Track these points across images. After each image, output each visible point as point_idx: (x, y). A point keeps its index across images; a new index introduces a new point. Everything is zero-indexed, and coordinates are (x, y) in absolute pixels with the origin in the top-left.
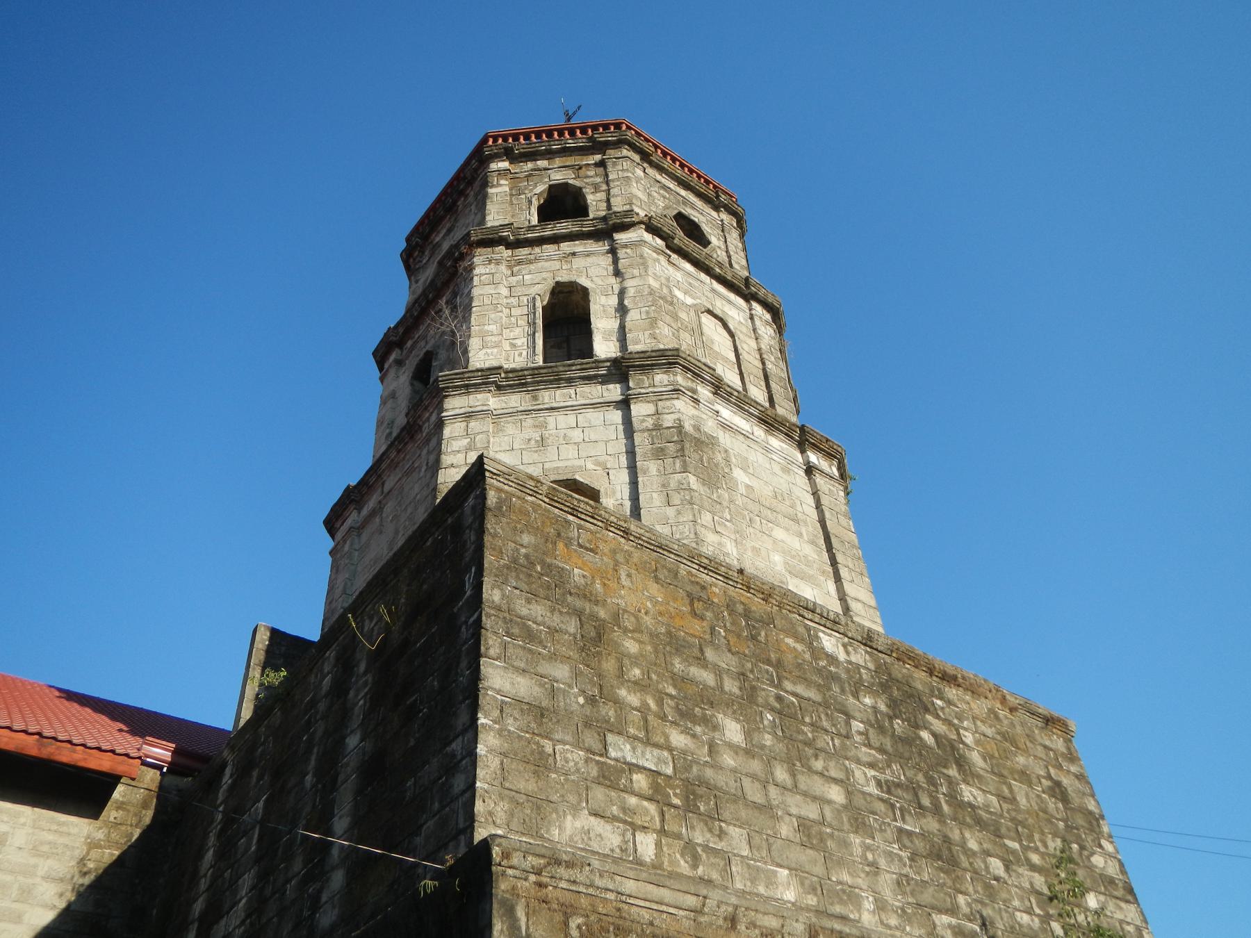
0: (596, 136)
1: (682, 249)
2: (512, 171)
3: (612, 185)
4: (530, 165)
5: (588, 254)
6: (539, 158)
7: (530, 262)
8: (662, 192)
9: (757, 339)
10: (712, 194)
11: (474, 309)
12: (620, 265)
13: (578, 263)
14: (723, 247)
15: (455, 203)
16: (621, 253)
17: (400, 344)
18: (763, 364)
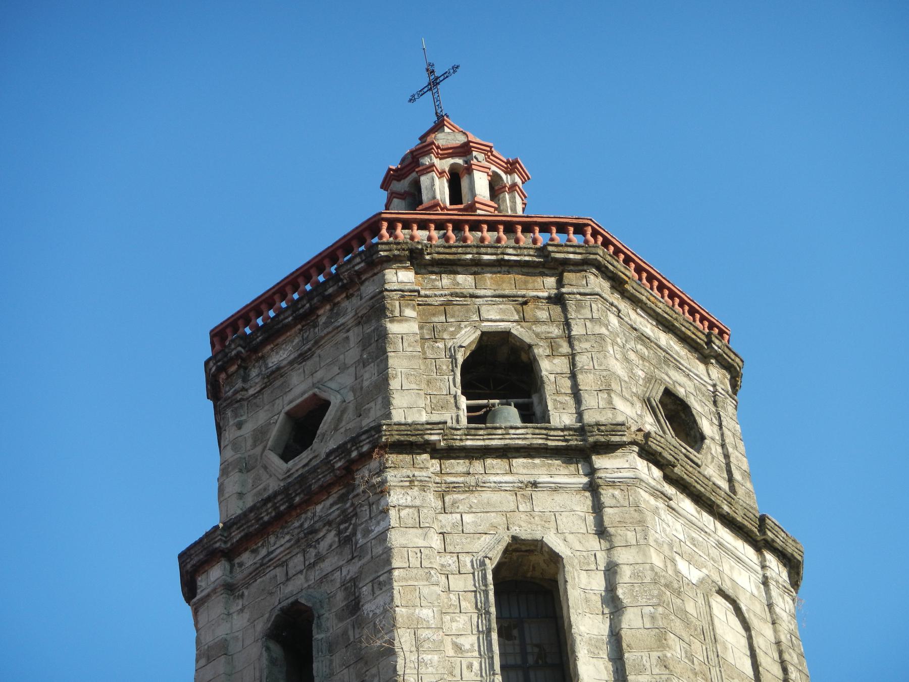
0: (550, 248)
1: (683, 479)
2: (423, 293)
3: (578, 346)
4: (446, 280)
5: (556, 489)
6: (459, 269)
7: (470, 489)
8: (639, 347)
9: (774, 623)
10: (701, 339)
11: (396, 573)
12: (607, 522)
13: (543, 501)
14: (717, 437)
15: (313, 310)
16: (607, 495)
17: (230, 555)
18: (785, 670)
